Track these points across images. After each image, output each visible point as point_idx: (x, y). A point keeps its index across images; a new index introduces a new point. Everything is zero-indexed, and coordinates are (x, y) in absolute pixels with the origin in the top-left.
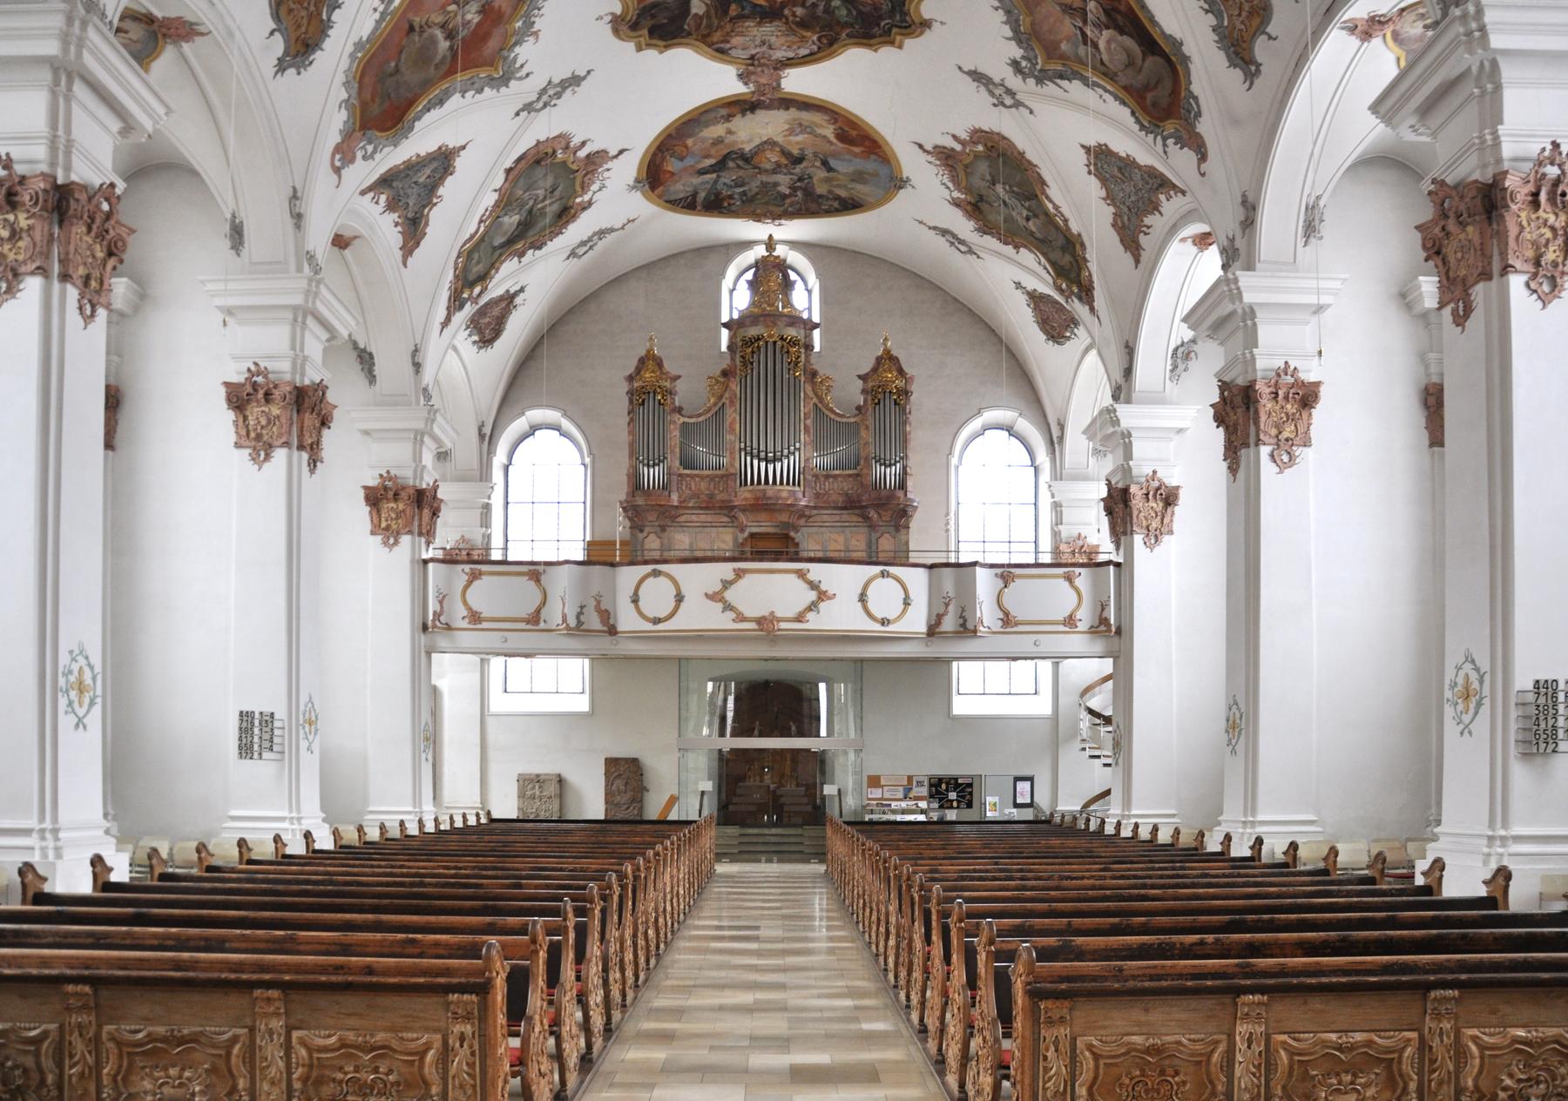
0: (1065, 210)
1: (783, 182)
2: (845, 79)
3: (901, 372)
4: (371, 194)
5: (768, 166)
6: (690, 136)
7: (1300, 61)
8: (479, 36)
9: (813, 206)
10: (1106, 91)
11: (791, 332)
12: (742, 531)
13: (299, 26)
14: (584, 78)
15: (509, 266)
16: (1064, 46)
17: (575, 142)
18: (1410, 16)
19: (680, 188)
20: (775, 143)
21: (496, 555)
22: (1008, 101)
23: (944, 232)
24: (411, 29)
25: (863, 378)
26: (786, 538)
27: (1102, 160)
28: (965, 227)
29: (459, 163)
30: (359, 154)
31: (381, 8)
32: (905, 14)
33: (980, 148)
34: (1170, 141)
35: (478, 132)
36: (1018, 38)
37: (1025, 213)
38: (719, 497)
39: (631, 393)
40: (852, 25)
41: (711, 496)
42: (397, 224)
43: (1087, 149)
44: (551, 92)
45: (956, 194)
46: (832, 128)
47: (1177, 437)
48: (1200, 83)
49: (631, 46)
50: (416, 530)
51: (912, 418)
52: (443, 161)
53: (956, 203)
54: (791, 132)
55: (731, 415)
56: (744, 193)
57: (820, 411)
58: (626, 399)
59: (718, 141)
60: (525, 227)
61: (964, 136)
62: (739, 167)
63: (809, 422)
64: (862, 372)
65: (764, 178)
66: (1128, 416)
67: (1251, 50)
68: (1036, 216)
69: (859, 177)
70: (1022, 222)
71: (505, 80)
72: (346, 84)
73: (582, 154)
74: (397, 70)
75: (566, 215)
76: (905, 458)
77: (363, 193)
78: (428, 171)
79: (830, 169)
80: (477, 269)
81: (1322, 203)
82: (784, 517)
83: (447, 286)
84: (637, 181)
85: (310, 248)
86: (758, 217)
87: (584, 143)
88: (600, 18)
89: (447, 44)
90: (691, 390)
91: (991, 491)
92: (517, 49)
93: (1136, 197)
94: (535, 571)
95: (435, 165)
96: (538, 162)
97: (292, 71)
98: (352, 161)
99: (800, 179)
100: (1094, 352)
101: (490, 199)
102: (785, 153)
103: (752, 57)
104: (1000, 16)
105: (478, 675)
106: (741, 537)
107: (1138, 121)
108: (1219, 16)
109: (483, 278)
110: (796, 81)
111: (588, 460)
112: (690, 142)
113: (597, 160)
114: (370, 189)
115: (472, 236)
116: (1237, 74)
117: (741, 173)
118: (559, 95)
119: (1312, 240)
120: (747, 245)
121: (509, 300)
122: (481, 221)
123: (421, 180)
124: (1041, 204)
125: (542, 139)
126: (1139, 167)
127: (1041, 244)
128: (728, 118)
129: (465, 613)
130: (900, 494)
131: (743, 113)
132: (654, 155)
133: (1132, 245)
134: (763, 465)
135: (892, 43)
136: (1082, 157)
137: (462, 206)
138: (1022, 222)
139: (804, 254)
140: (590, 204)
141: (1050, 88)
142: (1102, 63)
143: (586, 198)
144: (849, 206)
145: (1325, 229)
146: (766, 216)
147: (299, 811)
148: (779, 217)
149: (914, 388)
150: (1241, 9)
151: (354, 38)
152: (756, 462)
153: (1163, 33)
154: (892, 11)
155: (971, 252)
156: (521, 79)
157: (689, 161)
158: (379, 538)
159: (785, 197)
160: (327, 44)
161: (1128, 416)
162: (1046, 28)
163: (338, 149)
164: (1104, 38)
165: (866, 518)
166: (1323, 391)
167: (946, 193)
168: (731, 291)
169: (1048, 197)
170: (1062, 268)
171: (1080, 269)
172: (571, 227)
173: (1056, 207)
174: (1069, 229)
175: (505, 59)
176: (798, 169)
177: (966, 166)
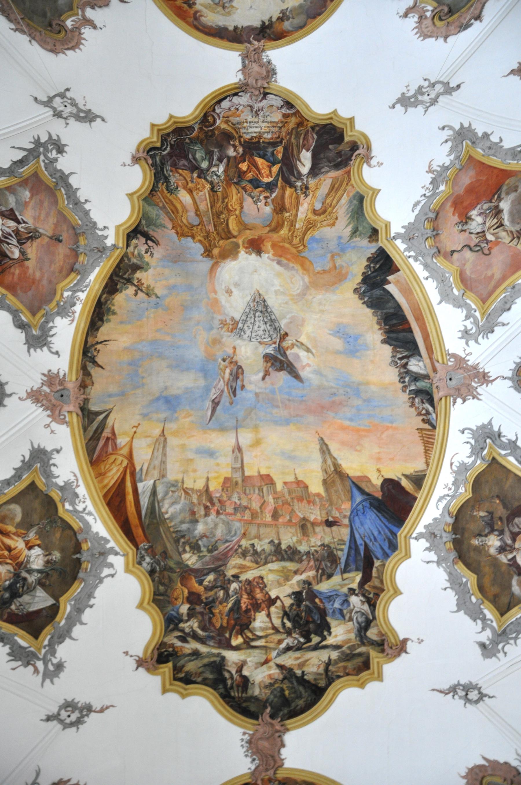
16: (27, 194)
36: (63, 178)
44: (426, 98)
88: (380, 164)
104: (82, 196)
118: (420, 91)
162: (46, 204)
175: (457, 158)
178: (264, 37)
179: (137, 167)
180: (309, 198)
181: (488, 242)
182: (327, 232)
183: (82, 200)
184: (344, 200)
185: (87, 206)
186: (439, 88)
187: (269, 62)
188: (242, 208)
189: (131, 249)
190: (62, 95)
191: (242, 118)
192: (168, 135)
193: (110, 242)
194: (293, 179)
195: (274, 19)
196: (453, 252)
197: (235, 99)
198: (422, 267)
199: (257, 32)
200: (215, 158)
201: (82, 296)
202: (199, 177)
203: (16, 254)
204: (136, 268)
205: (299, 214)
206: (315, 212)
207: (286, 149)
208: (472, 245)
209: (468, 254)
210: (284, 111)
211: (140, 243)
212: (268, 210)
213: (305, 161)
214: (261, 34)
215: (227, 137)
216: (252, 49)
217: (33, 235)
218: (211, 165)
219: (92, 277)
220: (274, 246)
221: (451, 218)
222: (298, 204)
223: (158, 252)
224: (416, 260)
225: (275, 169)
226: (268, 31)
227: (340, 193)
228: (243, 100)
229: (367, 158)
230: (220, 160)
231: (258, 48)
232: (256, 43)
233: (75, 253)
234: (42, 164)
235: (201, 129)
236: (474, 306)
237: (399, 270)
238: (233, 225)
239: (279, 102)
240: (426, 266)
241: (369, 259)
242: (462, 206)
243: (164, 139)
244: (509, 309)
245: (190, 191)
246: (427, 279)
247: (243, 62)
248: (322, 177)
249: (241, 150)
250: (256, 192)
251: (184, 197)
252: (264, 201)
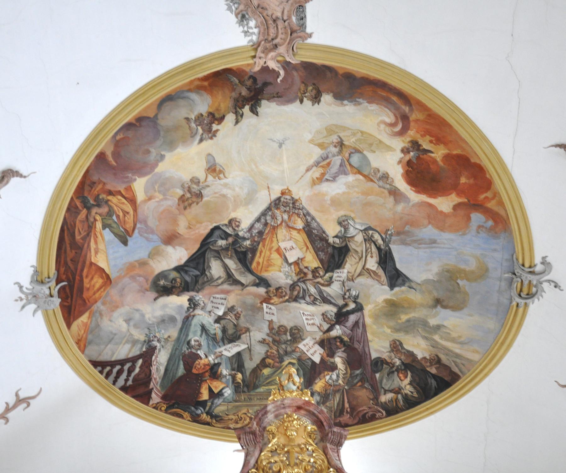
46: (398, 144)
54: (324, 170)
56: (238, 362)
59: (192, 195)
79: (396, 278)
102: (314, 236)
112: (139, 186)
117: (234, 297)
128: (210, 122)
132: (72, 209)
144: (433, 382)
157: (139, 248)
178: (253, 78)
187: (243, 16)
195: (230, 118)
199: (269, 90)
214: (259, 85)
216: (282, 50)
226: (244, 92)
231: (266, 51)
232: (272, 65)
247: (302, 19)
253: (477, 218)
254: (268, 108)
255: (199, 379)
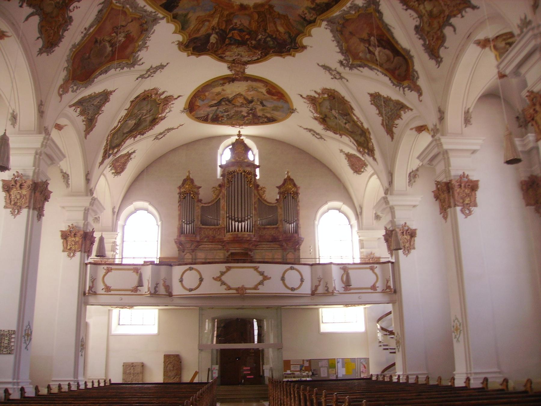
0: (362, 119)
1: (244, 111)
2: (272, 69)
3: (295, 185)
4: (74, 108)
5: (238, 104)
6: (207, 91)
7: (458, 58)
8: (124, 46)
9: (256, 121)
10: (378, 71)
11: (248, 169)
12: (228, 252)
13: (49, 37)
14: (166, 66)
15: (129, 141)
16: (361, 55)
17: (160, 91)
18: (500, 40)
19: (202, 113)
20: (242, 95)
21: (117, 261)
22: (338, 77)
23: (310, 130)
24: (96, 41)
25: (279, 187)
26: (246, 254)
27: (375, 98)
28: (319, 128)
29: (111, 97)
30: (70, 90)
31: (85, 32)
32: (296, 43)
33: (326, 96)
34: (406, 89)
35: (120, 86)
36: (342, 52)
37: (344, 121)
38: (218, 237)
39: (180, 193)
40: (275, 48)
41: (214, 237)
42: (83, 121)
43: (371, 95)
44: (152, 71)
45: (315, 115)
46: (265, 89)
47: (416, 208)
48: (417, 66)
49: (185, 54)
50: (83, 250)
51: (300, 204)
52: (105, 96)
53: (316, 118)
54: (248, 90)
55: (223, 203)
56: (228, 115)
57: (261, 201)
58: (178, 196)
59: (218, 94)
60: (137, 125)
61: (319, 91)
62: (226, 104)
63: (256, 206)
64: (279, 185)
65: (236, 109)
66: (393, 200)
67: (438, 52)
68: (349, 122)
69: (275, 109)
70: (343, 125)
71: (133, 65)
72: (67, 61)
73: (163, 97)
74: (89, 57)
75: (154, 122)
76: (298, 220)
77: (70, 106)
78: (98, 100)
79: (264, 106)
80: (116, 142)
81: (471, 111)
82: (246, 246)
83: (103, 147)
84: (185, 109)
85: (46, 125)
86: (233, 125)
87: (164, 92)
89: (111, 49)
90: (206, 194)
91: (335, 236)
92: (139, 53)
93: (390, 112)
94: (136, 269)
95: (101, 97)
96: (144, 99)
97: (45, 54)
98: (67, 92)
99: (251, 110)
100: (375, 177)
101: (124, 113)
102: (245, 99)
103: (234, 60)
104: (335, 43)
105: (107, 317)
106: (227, 254)
107: (392, 82)
108: (424, 40)
109: (119, 145)
110: (251, 70)
111: (160, 223)
112: (207, 94)
113: (168, 100)
114: (74, 105)
115: (115, 128)
116: (433, 62)
117: (227, 107)
118: (155, 72)
119: (468, 125)
120: (228, 136)
121: (129, 156)
122: (119, 122)
123: (95, 104)
124: (351, 117)
125: (147, 89)
126: (392, 101)
127: (351, 134)
128: (223, 84)
129: (103, 287)
130: (296, 235)
131: (229, 82)
133: (390, 132)
134: (237, 223)
135: (290, 55)
136: (369, 98)
137: (112, 115)
138: (343, 125)
139: (252, 140)
140: (165, 117)
141: (355, 71)
142: (377, 60)
143: (163, 115)
144: (271, 120)
145: (473, 121)
146: (236, 125)
147: (18, 379)
148: (242, 125)
149: (300, 191)
150: (433, 37)
151: (73, 43)
152: (233, 222)
153: (402, 48)
154: (291, 42)
155: (321, 138)
156: (140, 65)
157: (206, 102)
158: (66, 253)
159: (244, 117)
160: (61, 44)
161: (393, 200)
163: (61, 87)
164: (377, 51)
165: (282, 246)
166: (480, 184)
167: (311, 115)
168: (221, 155)
169: (354, 114)
170: (360, 142)
171: (368, 143)
172: (156, 127)
173: (358, 118)
174: (363, 127)
175: (134, 56)
176: (251, 105)
177: (320, 103)
179: (305, 44)
180: (212, 25)
181: (115, 32)
182: (202, 14)
183: (335, 42)
184: (192, 27)
185: (333, 39)
186: (147, 76)
188: (250, 22)
189: (314, 17)
190: (336, 78)
191: (246, 53)
192: (286, 52)
193: (324, 23)
194: (221, 32)
196: (132, 21)
197: (250, 59)
198: (148, 10)
200: (262, 41)
201: (345, 8)
202: (272, 35)
203: (372, 38)
204: (313, 9)
205: (217, 19)
206: (209, 21)
207: (224, 42)
208: (123, 28)
209: (124, 23)
210: (224, 55)
211: (308, 16)
212: (235, 21)
213: (213, 39)
215: (256, 47)
217: (362, 40)
218: (265, 39)
219: (337, 13)
220: (233, 7)
221: (134, 34)
222: (218, 23)
223: (300, 12)
224: (151, 12)
225: (230, 35)
227: (195, 28)
228: (245, 59)
229: (180, 44)
230: (260, 40)
233: (343, 26)
234: (351, 60)
235: (269, 51)
236: (118, 4)
237: (161, 6)
238: (256, 16)
239: (226, 58)
240: (145, 11)
241: (177, 6)
242: (130, 39)
243: (289, 51)
244: (99, 12)
245: (278, 31)
246: (144, 6)
248: (204, 34)
249: (248, 42)
250: (241, 28)
251: (281, 29)
252: (238, 24)
253: (281, 100)
254: (235, 82)
255: (219, 118)
